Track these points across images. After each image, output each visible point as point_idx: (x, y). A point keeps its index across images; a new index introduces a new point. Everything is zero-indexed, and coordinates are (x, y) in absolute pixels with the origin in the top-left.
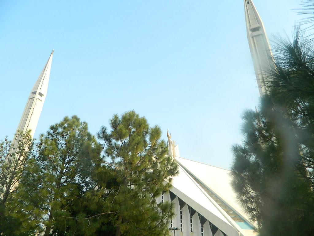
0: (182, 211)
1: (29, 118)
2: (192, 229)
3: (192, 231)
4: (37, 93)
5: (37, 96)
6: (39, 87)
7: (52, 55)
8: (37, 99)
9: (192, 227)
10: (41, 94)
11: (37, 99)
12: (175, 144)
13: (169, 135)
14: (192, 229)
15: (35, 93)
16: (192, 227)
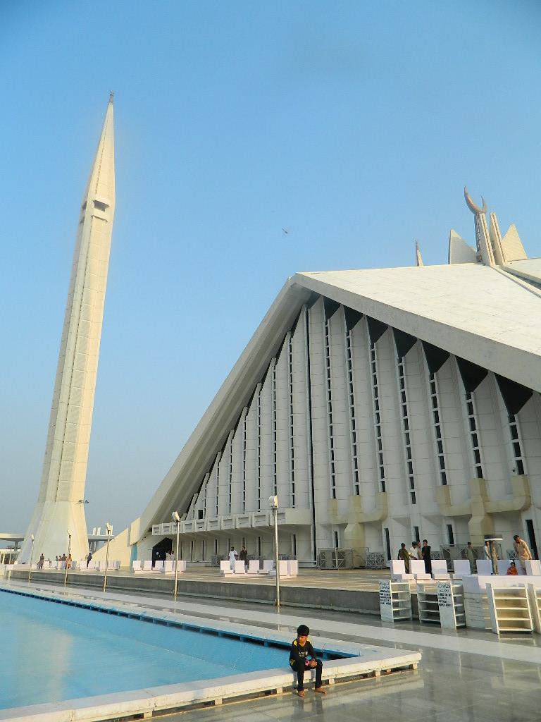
0: (472, 400)
1: (81, 265)
2: (520, 463)
3: (521, 471)
4: (90, 205)
5: (92, 210)
6: (92, 188)
7: (111, 109)
8: (92, 217)
9: (518, 453)
10: (100, 205)
11: (92, 217)
12: (495, 220)
13: (479, 207)
14: (520, 463)
15: (84, 207)
16: (518, 453)
